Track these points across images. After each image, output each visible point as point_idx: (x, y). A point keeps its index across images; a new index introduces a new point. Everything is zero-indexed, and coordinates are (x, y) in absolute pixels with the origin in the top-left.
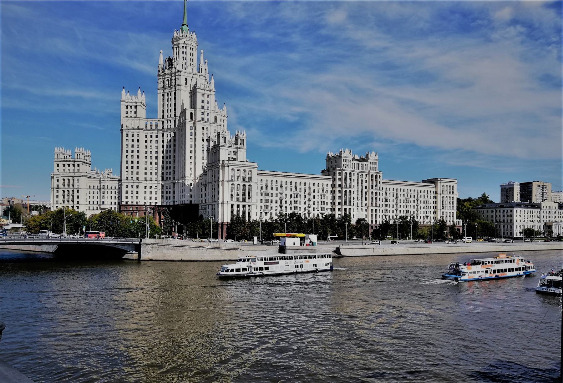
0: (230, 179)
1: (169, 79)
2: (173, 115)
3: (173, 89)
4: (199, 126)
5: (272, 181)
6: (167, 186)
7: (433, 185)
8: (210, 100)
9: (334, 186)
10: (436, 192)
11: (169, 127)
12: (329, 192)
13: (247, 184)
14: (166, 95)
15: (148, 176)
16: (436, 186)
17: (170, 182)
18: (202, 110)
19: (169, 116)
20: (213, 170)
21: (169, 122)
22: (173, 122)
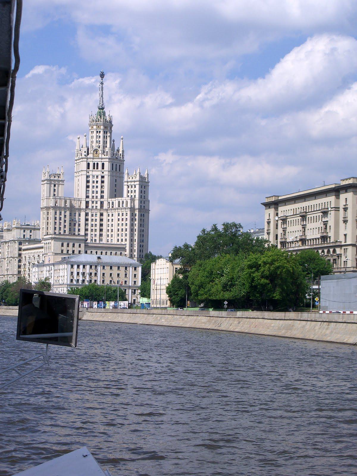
2: (99, 197)
11: (94, 208)
14: (91, 177)
21: (95, 202)
22: (99, 203)
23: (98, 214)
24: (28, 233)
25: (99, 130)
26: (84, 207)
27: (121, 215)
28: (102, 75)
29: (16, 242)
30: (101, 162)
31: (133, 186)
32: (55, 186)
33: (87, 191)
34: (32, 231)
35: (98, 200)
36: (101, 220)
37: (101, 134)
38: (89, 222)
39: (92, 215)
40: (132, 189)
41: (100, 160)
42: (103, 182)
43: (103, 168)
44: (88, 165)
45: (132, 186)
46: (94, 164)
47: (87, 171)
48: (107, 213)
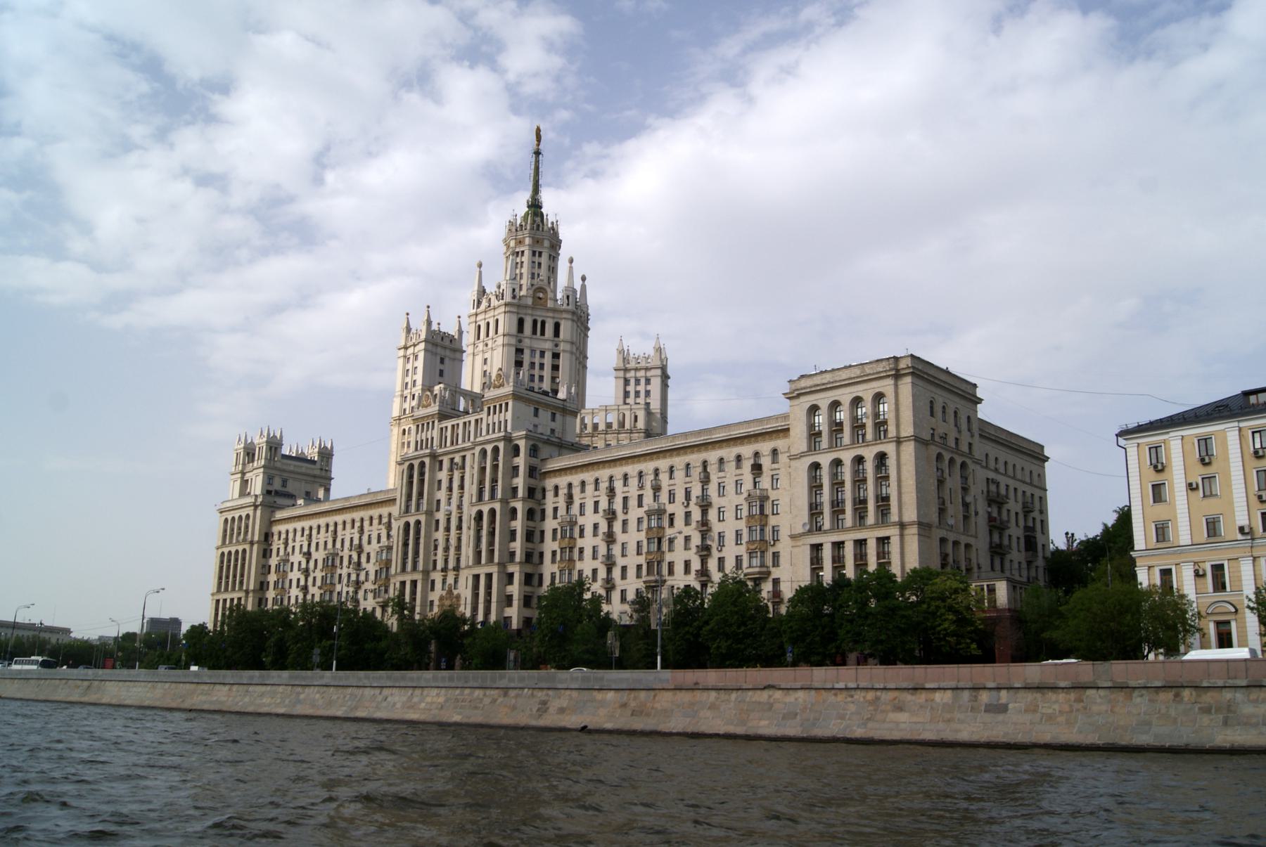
3: (548, 346)
14: (527, 353)
24: (545, 415)
25: (538, 249)
29: (522, 444)
31: (643, 381)
32: (442, 361)
34: (558, 416)
37: (544, 260)
40: (638, 388)
41: (551, 314)
42: (555, 368)
43: (557, 333)
44: (521, 323)
45: (637, 382)
46: (535, 322)
47: (517, 336)
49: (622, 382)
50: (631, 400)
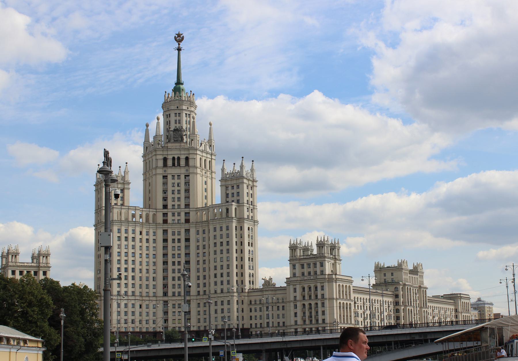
0: (338, 297)
1: (176, 158)
2: (183, 206)
4: (246, 226)
5: (358, 298)
6: (174, 305)
7: (452, 301)
8: (253, 192)
9: (397, 303)
10: (456, 310)
11: (176, 221)
12: (392, 311)
13: (349, 303)
14: (170, 177)
15: (144, 290)
16: (455, 304)
17: (179, 298)
18: (248, 205)
19: (176, 207)
20: (306, 286)
21: (176, 214)
22: (183, 214)
23: (183, 231)
25: (178, 112)
26: (162, 222)
27: (218, 229)
28: (179, 38)
30: (184, 154)
31: (235, 187)
33: (165, 199)
35: (182, 210)
36: (187, 240)
38: (170, 243)
39: (173, 234)
41: (182, 152)
44: (165, 160)
45: (233, 187)
46: (174, 158)
47: (162, 169)
48: (196, 229)
49: (224, 188)
50: (230, 199)
